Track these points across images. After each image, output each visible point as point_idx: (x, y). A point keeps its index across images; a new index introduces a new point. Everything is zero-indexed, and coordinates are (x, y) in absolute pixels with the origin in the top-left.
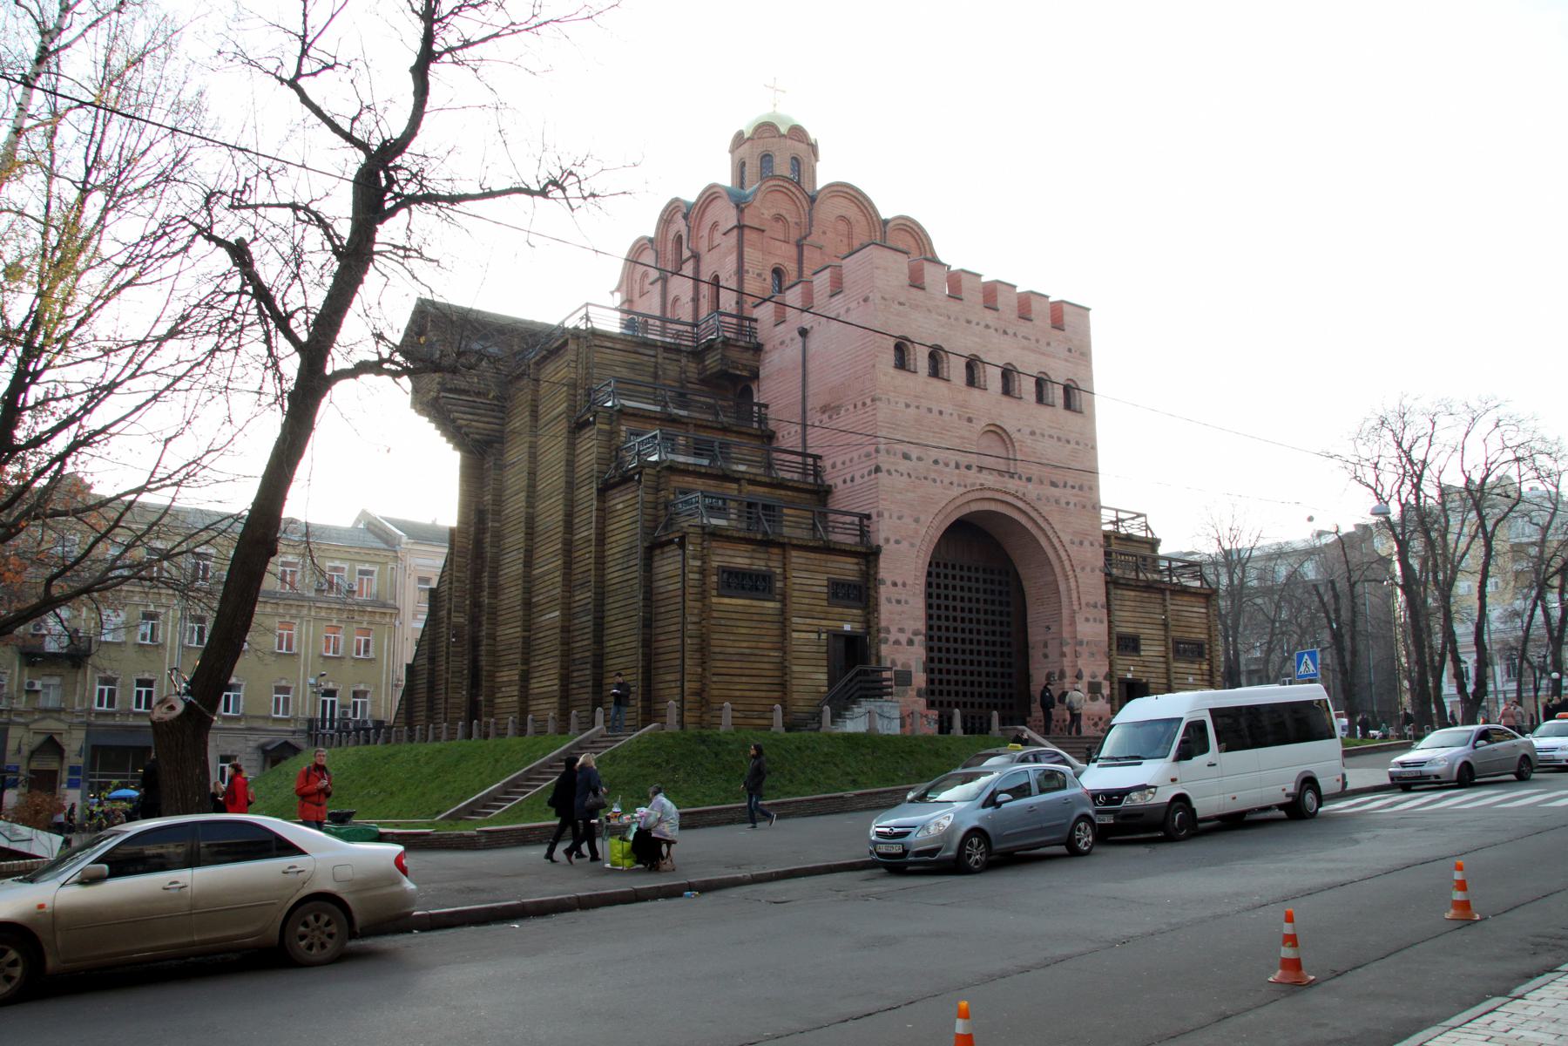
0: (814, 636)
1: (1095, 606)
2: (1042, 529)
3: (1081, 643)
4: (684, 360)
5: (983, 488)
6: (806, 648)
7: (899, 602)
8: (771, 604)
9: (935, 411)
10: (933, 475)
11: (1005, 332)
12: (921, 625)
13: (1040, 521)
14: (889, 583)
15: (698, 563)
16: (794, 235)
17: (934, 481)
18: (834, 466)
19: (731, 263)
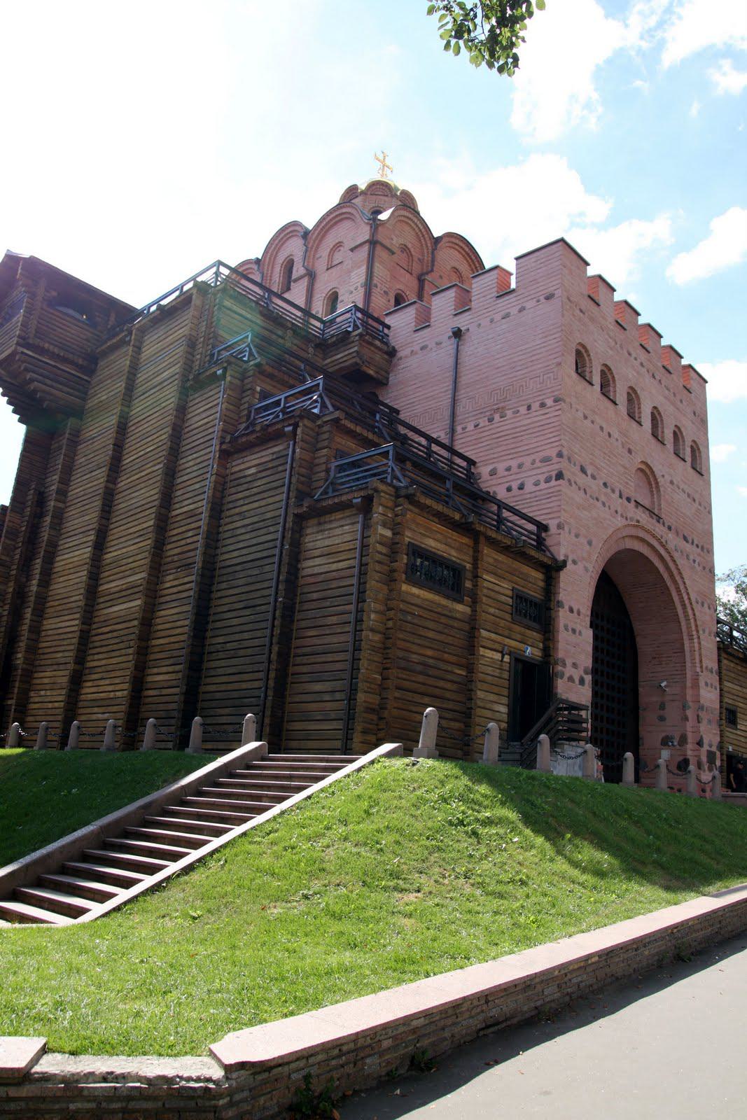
0: (498, 656)
1: (712, 672)
2: (675, 582)
3: (702, 708)
4: (311, 350)
6: (489, 670)
7: (574, 631)
8: (460, 607)
11: (653, 376)
12: (588, 662)
13: (675, 572)
14: (567, 607)
15: (388, 533)
16: (417, 269)
18: (493, 473)
19: (359, 275)
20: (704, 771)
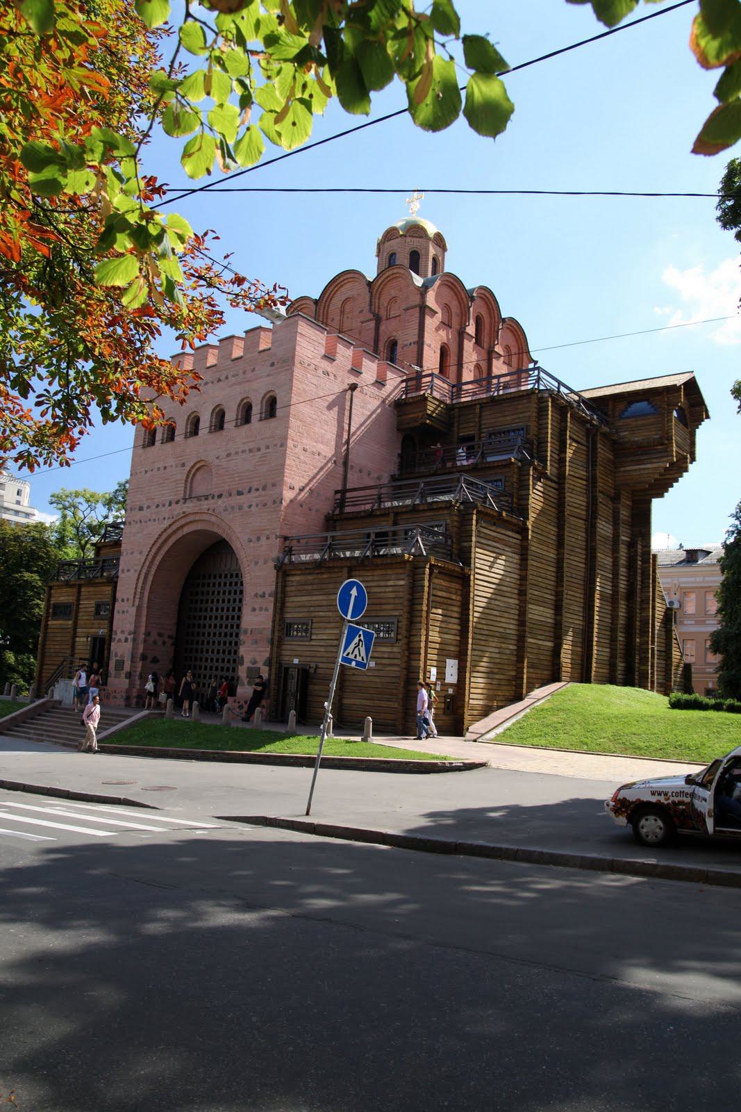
1: (263, 596)
3: (246, 632)
5: (186, 515)
7: (123, 612)
10: (154, 517)
14: (120, 600)
17: (155, 520)
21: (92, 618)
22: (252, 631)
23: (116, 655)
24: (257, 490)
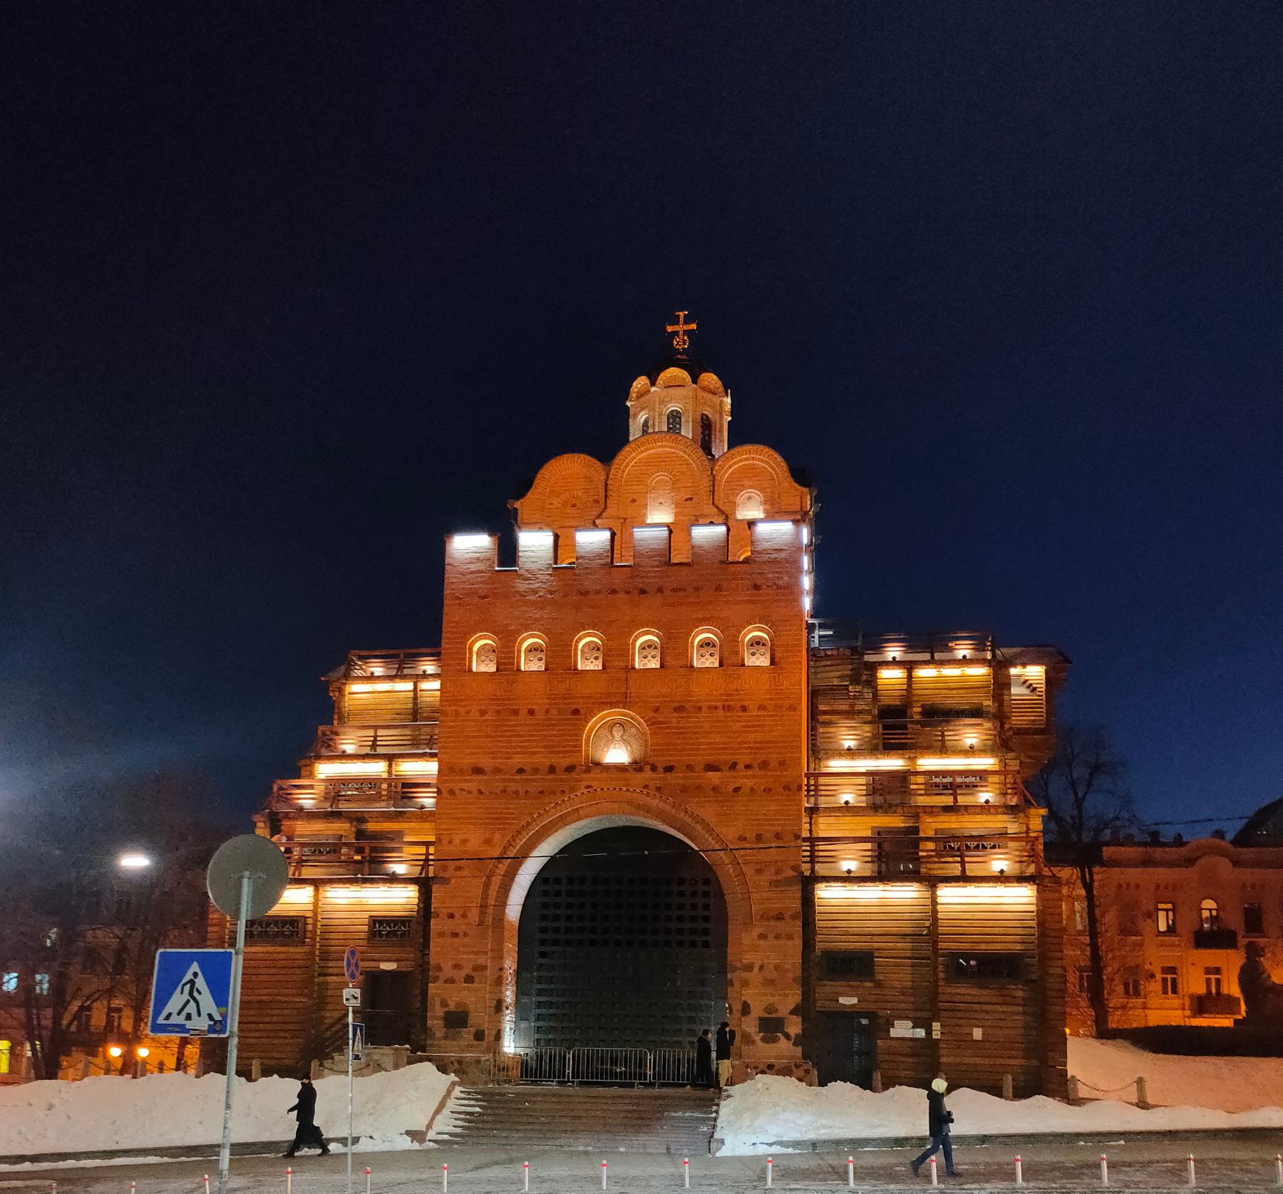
1: (779, 917)
3: (749, 968)
7: (455, 935)
9: (524, 712)
20: (753, 1042)
21: (365, 943)
22: (761, 967)
23: (444, 1004)
24: (748, 767)
